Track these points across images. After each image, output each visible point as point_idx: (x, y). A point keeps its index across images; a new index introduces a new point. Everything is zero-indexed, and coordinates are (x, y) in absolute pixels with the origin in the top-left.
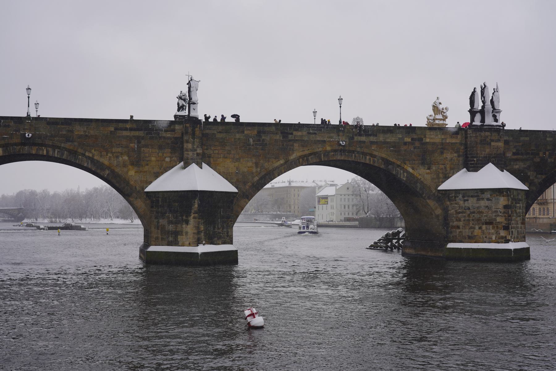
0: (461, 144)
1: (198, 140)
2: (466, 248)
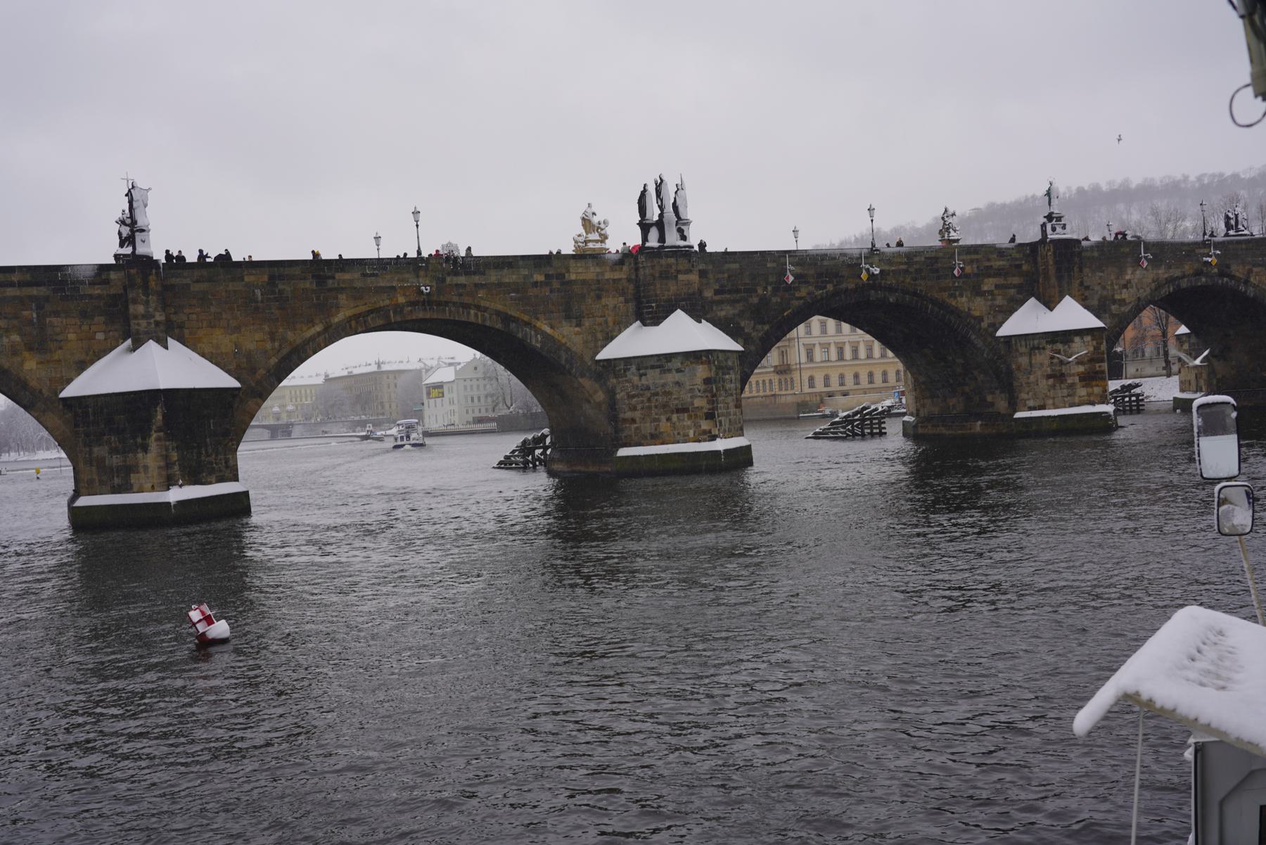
0: (629, 280)
1: (155, 298)
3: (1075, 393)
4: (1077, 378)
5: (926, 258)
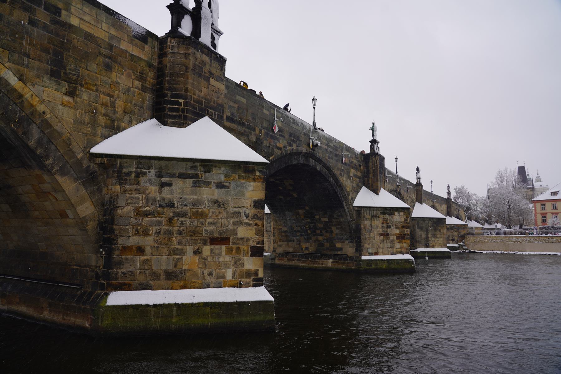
2: (160, 305)
3: (394, 246)
4: (395, 237)
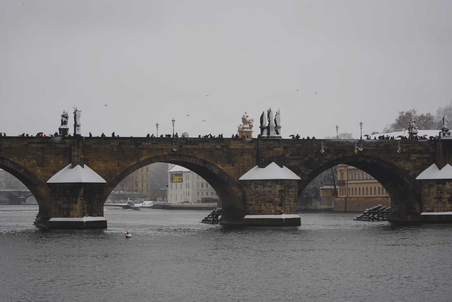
4: (447, 200)
5: (385, 145)
